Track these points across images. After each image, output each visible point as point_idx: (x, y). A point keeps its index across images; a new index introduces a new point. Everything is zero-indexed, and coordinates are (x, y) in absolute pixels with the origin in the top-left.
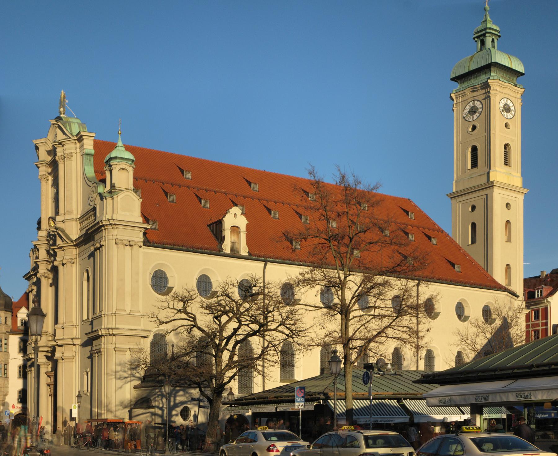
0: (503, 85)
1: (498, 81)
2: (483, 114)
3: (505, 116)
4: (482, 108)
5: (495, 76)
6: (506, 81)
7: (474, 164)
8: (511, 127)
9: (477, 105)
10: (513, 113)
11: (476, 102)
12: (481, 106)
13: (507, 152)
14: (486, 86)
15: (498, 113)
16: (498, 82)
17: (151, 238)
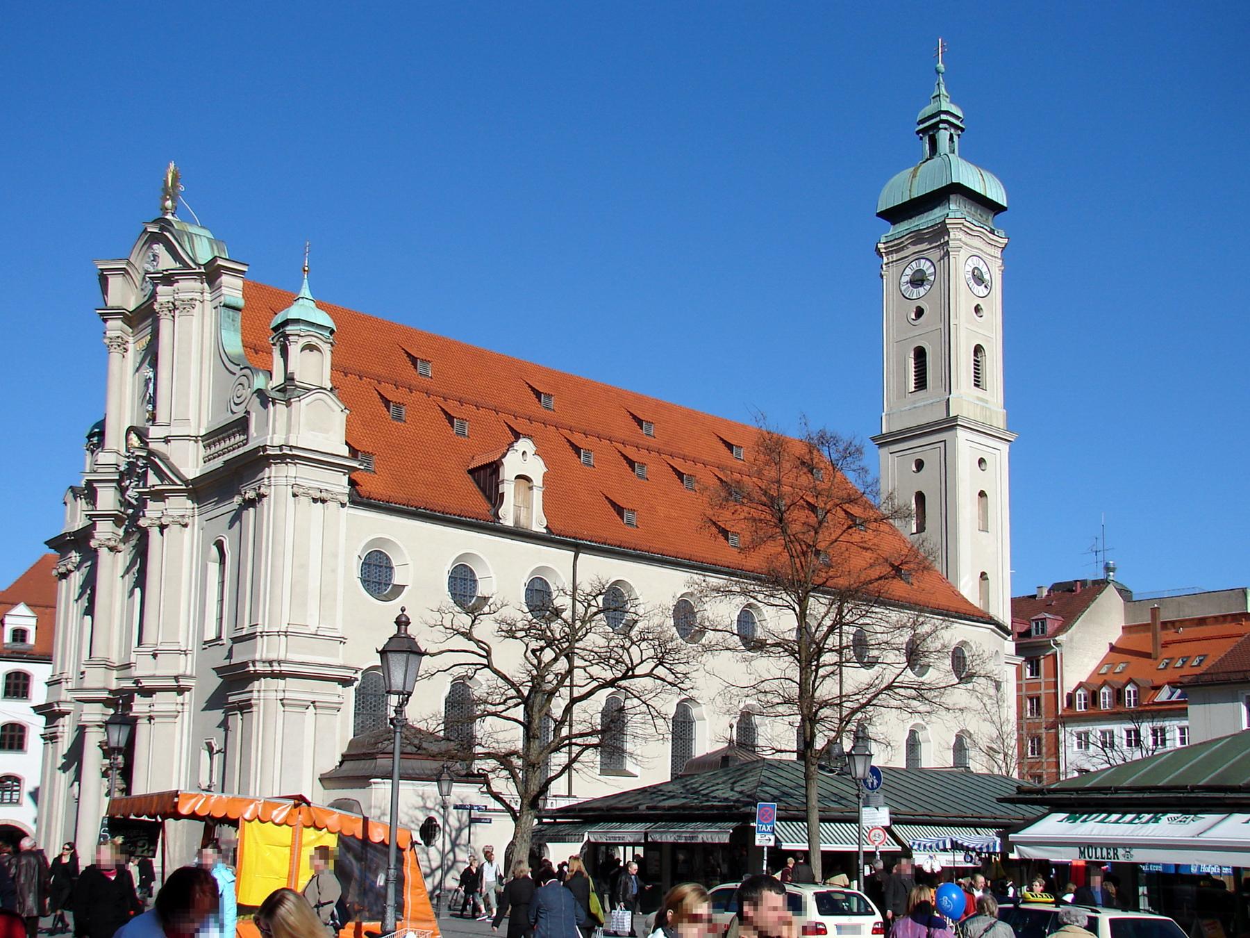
1: (963, 221)
2: (936, 285)
5: (958, 211)
8: (985, 312)
9: (925, 269)
12: (932, 270)
13: (978, 362)
14: (941, 231)
17: (370, 485)
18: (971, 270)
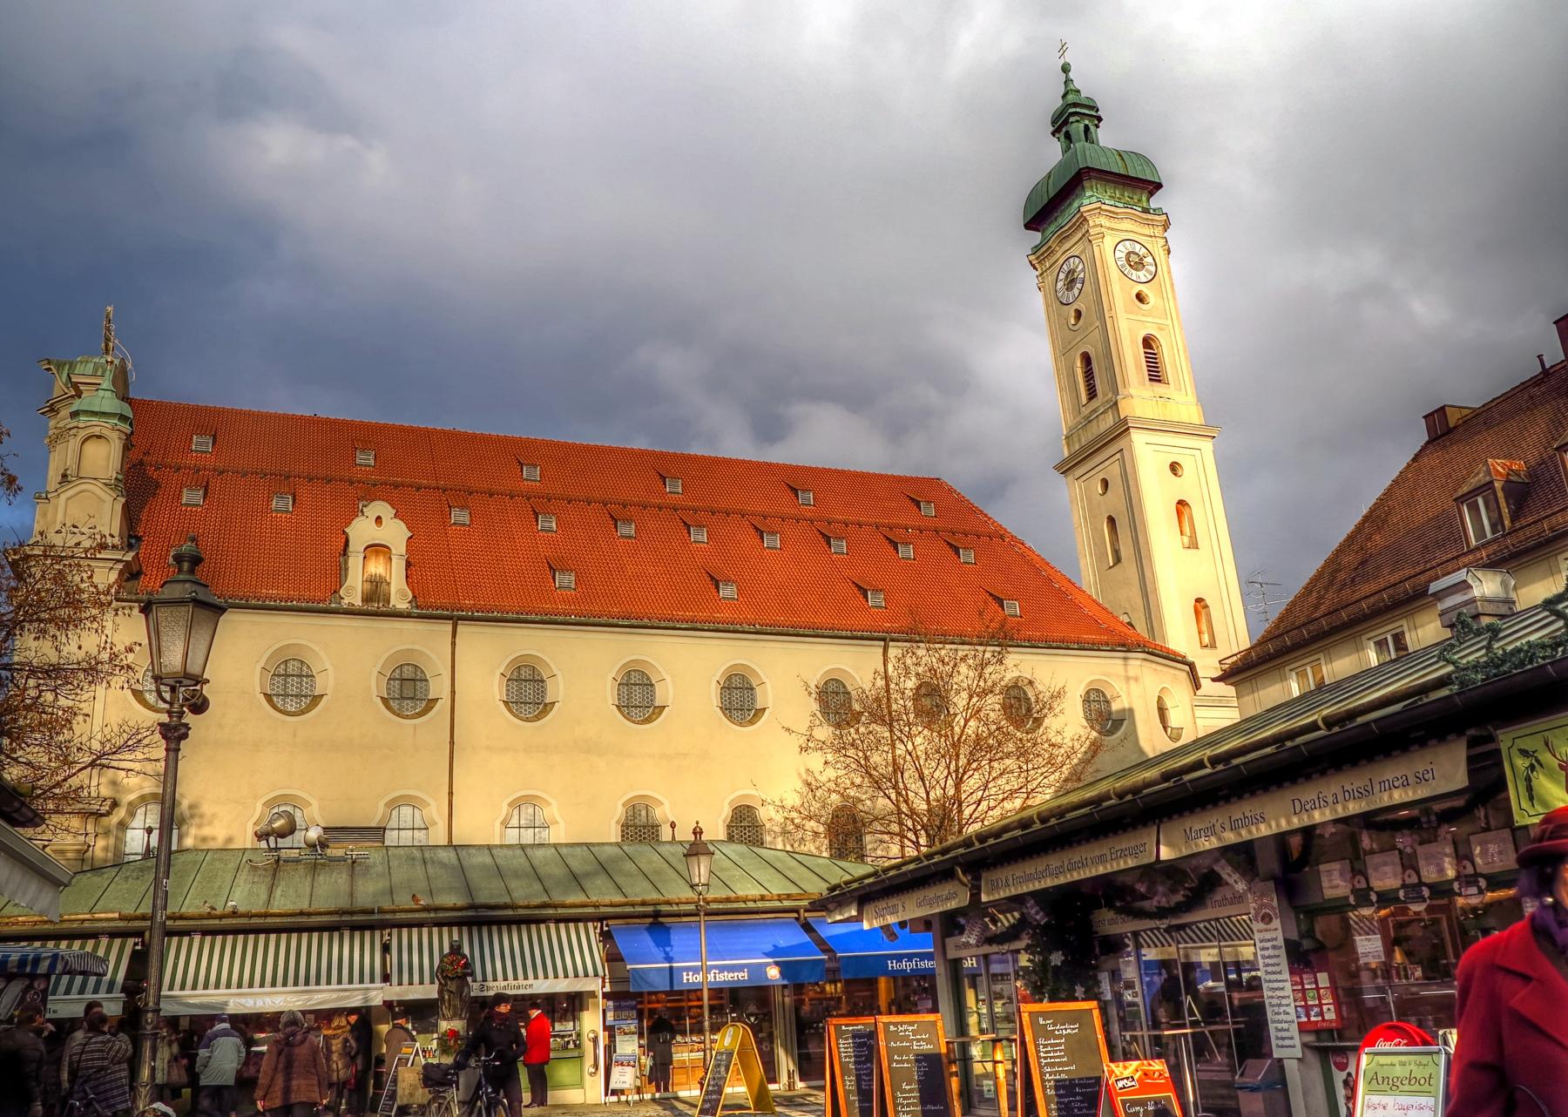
0: (1114, 213)
1: (1099, 205)
3: (1134, 278)
4: (1083, 270)
6: (1121, 205)
7: (1092, 394)
8: (1152, 298)
10: (1153, 269)
11: (1072, 260)
15: (1114, 274)
16: (1100, 208)
18: (1124, 255)
